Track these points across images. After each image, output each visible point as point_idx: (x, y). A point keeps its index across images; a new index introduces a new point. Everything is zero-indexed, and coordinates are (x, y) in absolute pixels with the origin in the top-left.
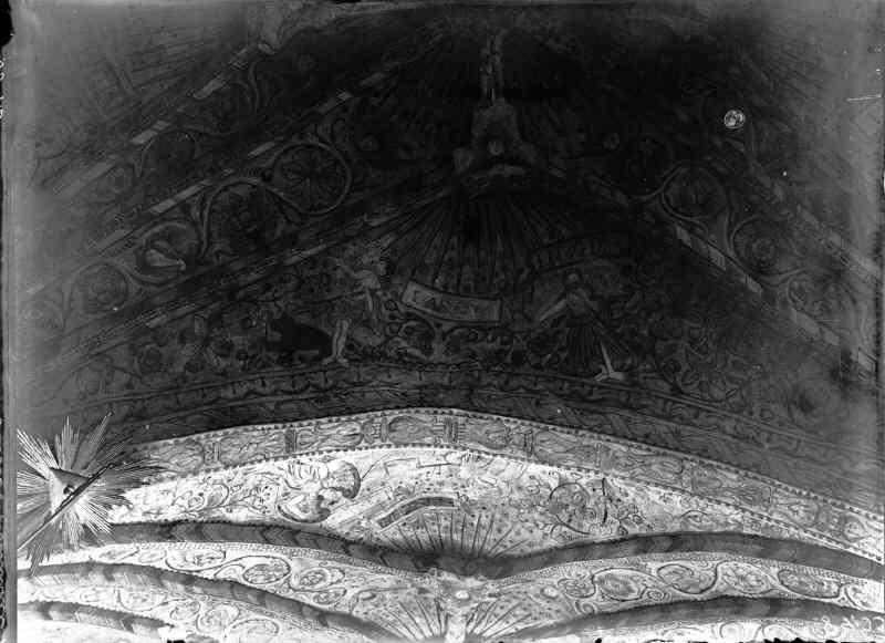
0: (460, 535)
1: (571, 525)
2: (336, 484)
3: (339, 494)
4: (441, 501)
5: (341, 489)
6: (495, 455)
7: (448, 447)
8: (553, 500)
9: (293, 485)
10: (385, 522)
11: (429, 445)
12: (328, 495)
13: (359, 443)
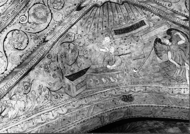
0: (110, 14)
1: (68, 44)
2: (164, 46)
3: (162, 41)
4: (117, 32)
5: (161, 43)
6: (113, 110)
7: (130, 106)
8: (77, 52)
9: (182, 52)
10: (142, 23)
11: (137, 106)
12: (167, 42)
13: (164, 109)
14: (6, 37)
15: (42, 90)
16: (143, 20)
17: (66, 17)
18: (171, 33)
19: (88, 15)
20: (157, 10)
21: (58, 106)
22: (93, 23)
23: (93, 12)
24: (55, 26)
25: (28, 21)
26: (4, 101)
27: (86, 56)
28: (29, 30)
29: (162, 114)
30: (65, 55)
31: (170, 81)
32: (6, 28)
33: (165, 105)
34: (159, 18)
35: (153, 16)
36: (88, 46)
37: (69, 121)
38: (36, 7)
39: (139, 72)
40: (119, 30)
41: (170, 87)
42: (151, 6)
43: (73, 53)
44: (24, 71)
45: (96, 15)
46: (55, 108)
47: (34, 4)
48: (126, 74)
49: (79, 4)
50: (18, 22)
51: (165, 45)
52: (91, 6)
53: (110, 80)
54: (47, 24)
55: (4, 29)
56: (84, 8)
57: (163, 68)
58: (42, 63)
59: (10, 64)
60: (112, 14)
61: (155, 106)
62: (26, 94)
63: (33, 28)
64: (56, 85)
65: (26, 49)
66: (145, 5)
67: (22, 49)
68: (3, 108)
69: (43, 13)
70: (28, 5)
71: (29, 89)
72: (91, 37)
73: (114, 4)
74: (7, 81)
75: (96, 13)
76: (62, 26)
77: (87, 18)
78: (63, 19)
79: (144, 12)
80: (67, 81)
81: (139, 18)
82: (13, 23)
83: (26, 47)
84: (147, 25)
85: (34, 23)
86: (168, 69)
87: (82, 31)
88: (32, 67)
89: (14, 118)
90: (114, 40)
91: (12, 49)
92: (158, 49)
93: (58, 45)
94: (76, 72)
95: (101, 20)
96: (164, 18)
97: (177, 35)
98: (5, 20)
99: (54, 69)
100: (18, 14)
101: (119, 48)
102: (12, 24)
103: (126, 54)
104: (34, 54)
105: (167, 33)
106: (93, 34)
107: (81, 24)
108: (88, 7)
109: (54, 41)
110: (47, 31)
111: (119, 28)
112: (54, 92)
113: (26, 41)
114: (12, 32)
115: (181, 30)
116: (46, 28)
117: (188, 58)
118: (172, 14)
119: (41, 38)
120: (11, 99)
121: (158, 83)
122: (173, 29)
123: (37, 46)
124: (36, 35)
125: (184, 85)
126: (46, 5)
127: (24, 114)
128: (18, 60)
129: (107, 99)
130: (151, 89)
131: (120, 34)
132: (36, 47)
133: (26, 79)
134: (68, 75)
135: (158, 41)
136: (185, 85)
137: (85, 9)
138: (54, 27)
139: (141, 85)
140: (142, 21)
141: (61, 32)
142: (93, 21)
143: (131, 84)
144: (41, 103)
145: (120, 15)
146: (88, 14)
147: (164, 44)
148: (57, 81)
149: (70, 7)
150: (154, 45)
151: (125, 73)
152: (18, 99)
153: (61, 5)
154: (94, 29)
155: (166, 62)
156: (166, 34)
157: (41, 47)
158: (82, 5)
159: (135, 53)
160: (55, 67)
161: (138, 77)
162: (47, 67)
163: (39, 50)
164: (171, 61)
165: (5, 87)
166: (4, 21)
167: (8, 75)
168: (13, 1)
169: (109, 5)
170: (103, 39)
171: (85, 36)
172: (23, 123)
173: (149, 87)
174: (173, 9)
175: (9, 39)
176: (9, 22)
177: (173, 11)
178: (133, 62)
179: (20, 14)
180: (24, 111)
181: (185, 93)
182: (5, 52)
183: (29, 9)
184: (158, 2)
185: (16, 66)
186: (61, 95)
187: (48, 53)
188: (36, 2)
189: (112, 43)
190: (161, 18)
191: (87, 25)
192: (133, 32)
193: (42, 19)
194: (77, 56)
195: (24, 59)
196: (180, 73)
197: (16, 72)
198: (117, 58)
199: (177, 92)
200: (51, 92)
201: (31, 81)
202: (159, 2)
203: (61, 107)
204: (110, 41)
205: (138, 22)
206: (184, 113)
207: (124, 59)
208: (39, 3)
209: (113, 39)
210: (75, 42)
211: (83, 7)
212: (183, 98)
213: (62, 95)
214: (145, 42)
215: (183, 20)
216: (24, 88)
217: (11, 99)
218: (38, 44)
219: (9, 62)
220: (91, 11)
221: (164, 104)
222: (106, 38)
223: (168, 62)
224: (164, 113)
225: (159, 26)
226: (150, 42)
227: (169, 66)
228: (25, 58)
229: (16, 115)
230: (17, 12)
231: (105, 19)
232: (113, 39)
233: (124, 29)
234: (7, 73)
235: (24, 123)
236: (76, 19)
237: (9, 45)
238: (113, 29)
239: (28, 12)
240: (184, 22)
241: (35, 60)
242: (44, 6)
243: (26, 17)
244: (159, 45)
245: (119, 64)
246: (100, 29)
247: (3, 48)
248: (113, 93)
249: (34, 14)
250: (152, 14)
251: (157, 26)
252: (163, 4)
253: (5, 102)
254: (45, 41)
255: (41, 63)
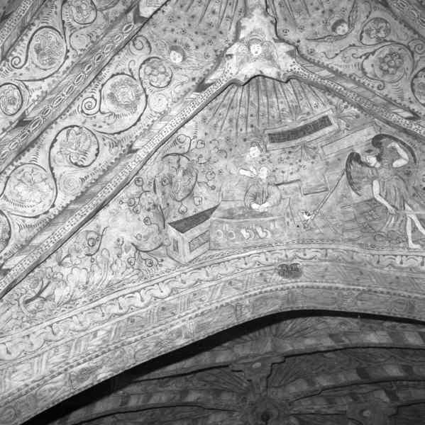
0: (261, 101)
1: (177, 158)
2: (366, 170)
3: (363, 159)
4: (275, 138)
5: (361, 163)
6: (261, 293)
7: (293, 287)
8: (194, 174)
9: (401, 183)
10: (325, 122)
11: (307, 287)
12: (372, 160)
14: (55, 140)
15: (123, 249)
16: (327, 117)
17: (175, 104)
18: (381, 144)
19: (217, 102)
20: (356, 95)
21: (154, 282)
22: (228, 118)
23: (228, 95)
24: (153, 121)
25: (100, 110)
26: (47, 268)
27: (211, 184)
28: (100, 127)
29: (356, 303)
30: (169, 181)
31: (375, 239)
32: (55, 121)
33: (363, 286)
34: (359, 112)
35: (346, 107)
36: (216, 165)
37: (174, 312)
38: (116, 81)
39: (315, 220)
40: (279, 134)
41: (374, 252)
42: (343, 87)
43: (187, 177)
44: (88, 209)
45: (235, 102)
46: (148, 284)
47: (113, 76)
48: (288, 223)
49: (201, 78)
50: (80, 110)
51: (368, 166)
52: (224, 83)
53: (256, 233)
54: (136, 117)
55: (53, 123)
56: (212, 87)
57: (362, 213)
58: (124, 195)
59: (61, 195)
60: (266, 101)
61: (343, 289)
62: (92, 255)
63: (108, 124)
64: (150, 240)
65: (93, 166)
66: (332, 85)
67: (85, 165)
68: (46, 282)
69: (130, 93)
70: (100, 77)
71: (97, 246)
72: (223, 146)
73: (271, 81)
74: (54, 229)
75: (235, 99)
76: (166, 122)
77: (215, 106)
78: (168, 108)
79: (328, 100)
80: (172, 232)
81: (318, 111)
82: (70, 112)
83: (94, 161)
84: (335, 126)
85: (112, 114)
86: (371, 215)
87: (206, 134)
88: (104, 202)
89: (66, 303)
90: (268, 154)
91: (67, 164)
92: (354, 174)
93: (157, 160)
94: (191, 215)
95: (243, 111)
96: (369, 113)
97: (394, 149)
98: (54, 106)
99: (147, 207)
100: (80, 95)
101: (277, 169)
102: (68, 114)
103: (291, 182)
104: (108, 177)
105: (373, 143)
106: (228, 139)
107: (204, 119)
108: (219, 86)
109: (150, 151)
110: (136, 131)
111: (279, 130)
112: (145, 253)
113: (93, 149)
114: (66, 130)
115: (400, 139)
116: (135, 125)
117: (412, 194)
118: (384, 106)
119: (125, 145)
120: (60, 264)
121: (350, 243)
122: (386, 136)
123: (116, 159)
124: (115, 138)
125: (401, 249)
126: (137, 77)
127: (85, 296)
128: (76, 186)
129: (249, 271)
130: (336, 254)
131: (279, 141)
132: (113, 161)
133: (91, 226)
134: (174, 220)
135: (354, 157)
136: (403, 248)
137: (213, 90)
138: (150, 123)
139: (317, 246)
140: (324, 117)
141: (164, 134)
142: (229, 114)
143: (298, 243)
144: (120, 274)
145: (282, 103)
146: (220, 99)
147: (367, 165)
148: (153, 232)
149: (182, 84)
150: (347, 165)
151: (287, 219)
152: (75, 266)
153: (164, 80)
154: (229, 129)
155: (369, 201)
156: (371, 145)
157: (122, 163)
158: (208, 81)
159: (309, 181)
160: (150, 203)
161: (311, 229)
162: (133, 203)
163: (119, 167)
164: (379, 199)
165: (49, 240)
166: (52, 107)
167: (56, 217)
168: (71, 68)
169: (261, 83)
170: (247, 151)
171: (211, 142)
172: (82, 313)
173: (333, 249)
174: (386, 95)
175: (61, 144)
176: (61, 112)
177: (385, 100)
178: (304, 199)
179: (85, 95)
180: (85, 288)
181: (403, 266)
182: (52, 169)
183: (103, 85)
184: (357, 79)
185: (73, 198)
186: (159, 259)
187: (136, 174)
188: (117, 71)
189: (263, 160)
190: (362, 112)
191: (215, 121)
192: (307, 138)
193: (127, 106)
194: (193, 182)
195: (89, 186)
196: (394, 225)
197: (73, 212)
198: (274, 189)
199: (388, 262)
200: (139, 254)
201: (101, 230)
202: (359, 81)
203: (158, 284)
204: (261, 156)
205: (315, 118)
206: (400, 303)
207: (286, 193)
208: (123, 74)
209: (267, 151)
210: (191, 154)
211: (210, 85)
212: (398, 274)
213: (162, 260)
214: (330, 161)
215: (406, 119)
216: (87, 242)
217: (60, 264)
218: (118, 156)
219: (58, 190)
220: (224, 94)
221: (361, 284)
222: (252, 148)
223: (372, 202)
224: (359, 302)
225: (356, 129)
226: (339, 159)
227: (374, 209)
228: (91, 183)
229: (69, 297)
230: (78, 91)
231: (253, 111)
232: (267, 151)
233: (289, 131)
234: (54, 211)
235: (84, 313)
236: (195, 109)
237: (60, 157)
238: (266, 132)
239: (100, 91)
240: (408, 122)
241: (111, 189)
242: (133, 80)
243: (96, 100)
244: (356, 166)
245: (275, 201)
246: (241, 130)
247: (47, 161)
248: (262, 258)
249: (112, 96)
250: (346, 104)
251: (352, 128)
252: (369, 84)
253: (49, 270)
254: (131, 150)
255: (122, 194)
